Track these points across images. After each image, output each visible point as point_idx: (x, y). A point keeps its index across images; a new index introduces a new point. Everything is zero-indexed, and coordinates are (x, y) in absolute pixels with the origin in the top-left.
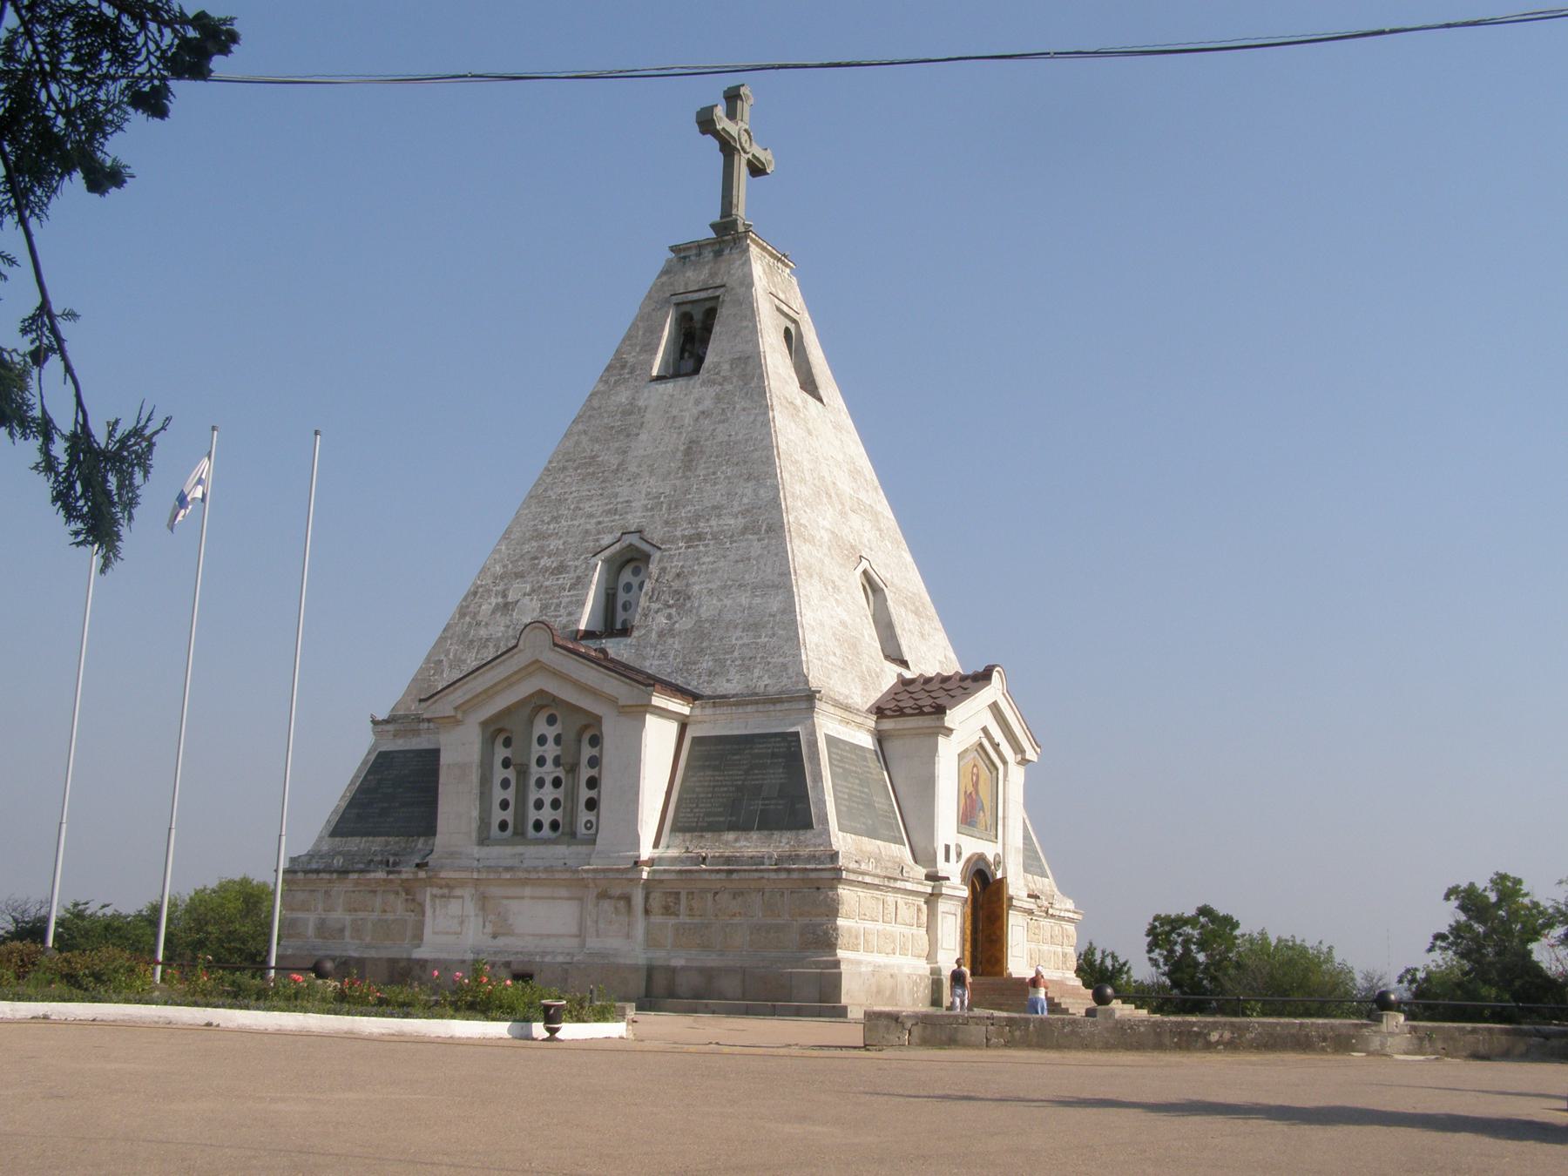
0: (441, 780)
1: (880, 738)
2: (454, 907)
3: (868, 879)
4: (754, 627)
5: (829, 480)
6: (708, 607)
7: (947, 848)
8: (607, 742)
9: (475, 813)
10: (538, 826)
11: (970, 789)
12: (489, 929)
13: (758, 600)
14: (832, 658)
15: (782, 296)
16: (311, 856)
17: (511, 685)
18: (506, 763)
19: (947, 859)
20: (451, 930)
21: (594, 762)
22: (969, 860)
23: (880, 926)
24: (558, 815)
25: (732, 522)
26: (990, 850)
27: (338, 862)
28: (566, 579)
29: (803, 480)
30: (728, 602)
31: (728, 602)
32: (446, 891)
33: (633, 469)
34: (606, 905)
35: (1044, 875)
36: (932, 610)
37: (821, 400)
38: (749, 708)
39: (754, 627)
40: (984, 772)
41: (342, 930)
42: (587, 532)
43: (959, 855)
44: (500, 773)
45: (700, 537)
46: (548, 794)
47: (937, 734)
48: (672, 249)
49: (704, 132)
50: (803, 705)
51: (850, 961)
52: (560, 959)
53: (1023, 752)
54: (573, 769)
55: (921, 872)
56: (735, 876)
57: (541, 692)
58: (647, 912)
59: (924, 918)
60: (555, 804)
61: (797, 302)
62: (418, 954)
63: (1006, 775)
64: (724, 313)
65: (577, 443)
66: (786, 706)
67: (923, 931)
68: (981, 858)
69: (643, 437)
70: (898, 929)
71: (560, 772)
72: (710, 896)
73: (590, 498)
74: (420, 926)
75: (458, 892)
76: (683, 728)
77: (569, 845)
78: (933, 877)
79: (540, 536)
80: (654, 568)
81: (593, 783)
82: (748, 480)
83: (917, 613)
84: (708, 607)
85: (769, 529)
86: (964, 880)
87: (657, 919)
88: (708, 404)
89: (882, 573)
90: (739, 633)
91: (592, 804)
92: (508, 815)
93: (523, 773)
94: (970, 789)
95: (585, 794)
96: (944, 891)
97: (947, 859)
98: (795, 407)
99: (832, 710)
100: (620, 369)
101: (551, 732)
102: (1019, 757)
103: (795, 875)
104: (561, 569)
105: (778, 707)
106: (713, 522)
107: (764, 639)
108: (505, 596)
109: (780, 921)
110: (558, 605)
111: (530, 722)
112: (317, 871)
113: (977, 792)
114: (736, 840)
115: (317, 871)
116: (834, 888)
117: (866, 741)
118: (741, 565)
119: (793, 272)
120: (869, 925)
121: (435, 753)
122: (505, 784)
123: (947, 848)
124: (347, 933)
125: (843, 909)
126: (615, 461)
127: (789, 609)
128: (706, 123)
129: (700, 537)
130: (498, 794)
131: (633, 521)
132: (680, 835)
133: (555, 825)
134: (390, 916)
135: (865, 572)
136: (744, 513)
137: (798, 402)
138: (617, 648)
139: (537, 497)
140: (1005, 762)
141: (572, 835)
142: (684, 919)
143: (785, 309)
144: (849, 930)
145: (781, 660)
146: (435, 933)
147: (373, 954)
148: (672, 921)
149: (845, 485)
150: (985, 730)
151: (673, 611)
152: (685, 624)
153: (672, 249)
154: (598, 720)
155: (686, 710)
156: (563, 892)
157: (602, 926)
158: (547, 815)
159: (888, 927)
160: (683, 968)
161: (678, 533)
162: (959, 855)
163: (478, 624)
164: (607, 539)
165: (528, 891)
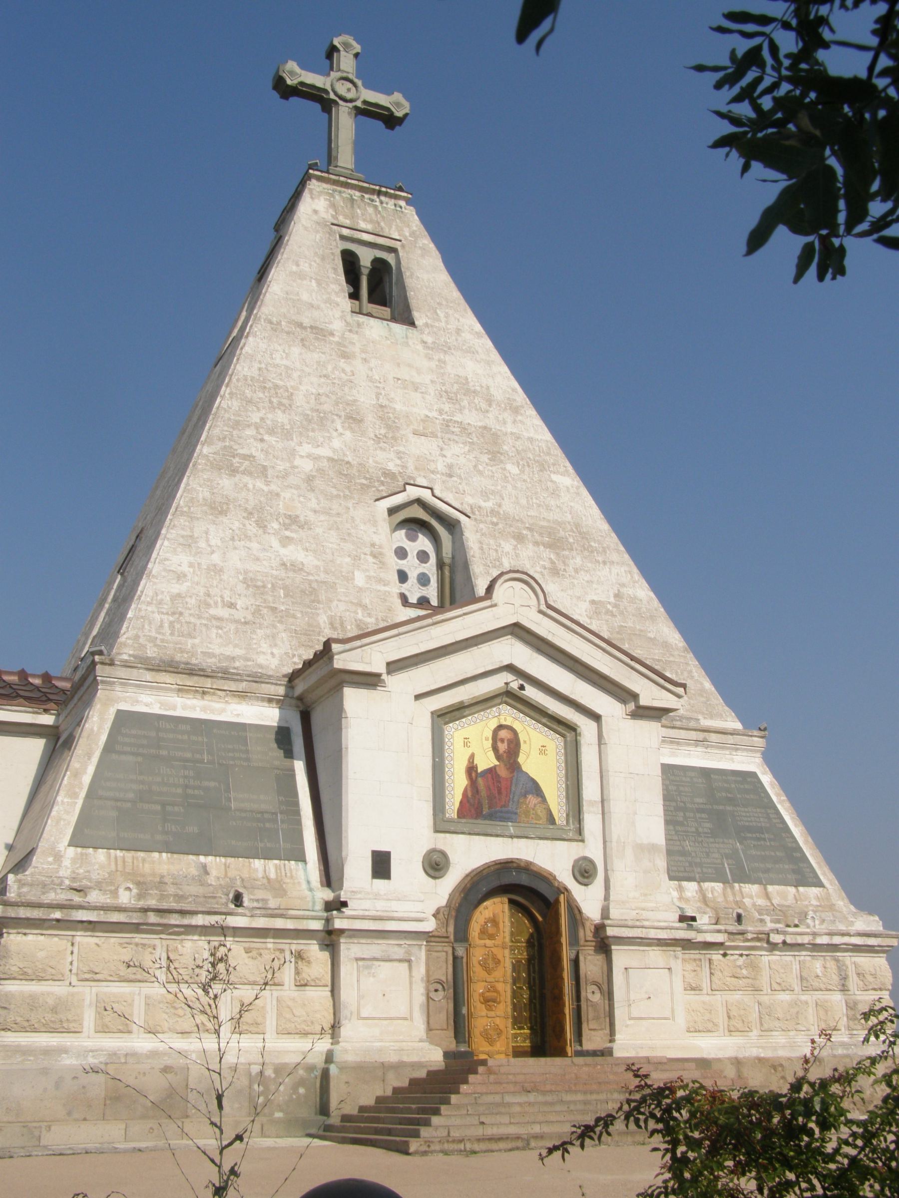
11: (486, 761)
15: (363, 225)
29: (286, 408)
36: (613, 540)
53: (635, 696)
89: (449, 497)
94: (486, 761)
99: (149, 676)
102: (632, 706)
113: (514, 766)
119: (408, 202)
137: (337, 326)
155: (48, 719)
162: (435, 865)
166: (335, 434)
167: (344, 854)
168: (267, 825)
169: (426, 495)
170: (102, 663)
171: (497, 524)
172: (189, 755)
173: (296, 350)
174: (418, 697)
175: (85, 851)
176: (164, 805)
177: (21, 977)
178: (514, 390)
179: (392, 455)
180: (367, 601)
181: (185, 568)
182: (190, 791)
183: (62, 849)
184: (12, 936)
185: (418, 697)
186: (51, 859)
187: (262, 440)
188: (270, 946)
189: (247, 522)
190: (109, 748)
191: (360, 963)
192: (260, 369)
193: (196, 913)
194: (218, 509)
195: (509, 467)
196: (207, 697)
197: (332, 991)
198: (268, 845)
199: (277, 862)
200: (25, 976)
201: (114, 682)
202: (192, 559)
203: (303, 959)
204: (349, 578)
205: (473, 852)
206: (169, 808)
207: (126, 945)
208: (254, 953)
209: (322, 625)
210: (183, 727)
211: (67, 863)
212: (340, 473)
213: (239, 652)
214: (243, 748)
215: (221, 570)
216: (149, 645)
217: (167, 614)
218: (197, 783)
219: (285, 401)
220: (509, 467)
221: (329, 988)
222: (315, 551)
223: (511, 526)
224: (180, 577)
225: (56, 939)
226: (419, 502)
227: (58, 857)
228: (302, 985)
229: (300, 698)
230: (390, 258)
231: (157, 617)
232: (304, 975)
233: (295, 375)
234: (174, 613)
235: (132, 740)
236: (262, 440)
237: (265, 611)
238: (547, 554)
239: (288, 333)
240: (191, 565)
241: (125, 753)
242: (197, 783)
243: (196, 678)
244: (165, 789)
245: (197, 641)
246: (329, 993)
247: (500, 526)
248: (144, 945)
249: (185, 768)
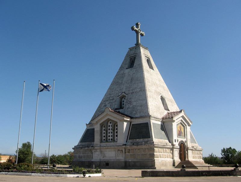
0: (95, 133)
2: (97, 153)
4: (141, 106)
5: (154, 82)
6: (134, 104)
7: (175, 140)
8: (118, 126)
9: (100, 138)
10: (109, 139)
12: (102, 156)
14: (154, 110)
15: (146, 54)
16: (77, 146)
17: (104, 118)
18: (104, 130)
19: (175, 142)
20: (97, 156)
21: (117, 129)
22: (180, 142)
23: (163, 153)
24: (112, 138)
25: (138, 90)
26: (184, 140)
27: (81, 146)
28: (114, 101)
29: (149, 82)
30: (137, 102)
31: (137, 102)
32: (96, 150)
33: (123, 83)
34: (119, 152)
35: (196, 143)
36: (174, 102)
37: (153, 70)
39: (141, 106)
40: (182, 127)
41: (82, 157)
42: (117, 93)
43: (178, 141)
44: (104, 132)
45: (133, 92)
46: (110, 134)
48: (129, 49)
49: (132, 30)
50: (149, 118)
51: (157, 160)
52: (113, 161)
54: (114, 130)
57: (108, 118)
58: (125, 153)
60: (112, 136)
61: (149, 55)
62: (93, 160)
63: (186, 128)
64: (137, 57)
65: (116, 80)
67: (171, 154)
68: (182, 141)
70: (166, 154)
71: (112, 131)
72: (135, 150)
73: (117, 88)
74: (93, 156)
75: (97, 151)
77: (113, 142)
79: (110, 94)
80: (126, 98)
81: (117, 132)
82: (140, 83)
83: (171, 102)
84: (134, 104)
85: (143, 90)
86: (179, 145)
87: (127, 154)
88: (134, 72)
89: (165, 96)
90: (139, 107)
91: (117, 136)
92: (105, 138)
93: (107, 131)
94: (179, 130)
95: (116, 134)
97: (175, 142)
98: (149, 71)
100: (121, 68)
101: (111, 125)
103: (147, 146)
104: (113, 99)
106: (135, 90)
107: (143, 108)
108: (105, 104)
109: (145, 153)
111: (107, 123)
112: (78, 148)
113: (181, 130)
115: (78, 148)
120: (161, 153)
121: (94, 129)
122: (104, 133)
123: (175, 140)
124: (83, 157)
125: (155, 151)
128: (132, 29)
129: (133, 92)
130: (103, 135)
131: (124, 91)
133: (112, 139)
134: (88, 155)
135: (161, 96)
136: (140, 88)
137: (149, 70)
138: (121, 110)
139: (110, 88)
140: (186, 125)
141: (114, 141)
142: (131, 153)
143: (147, 56)
145: (145, 111)
146: (95, 157)
147: (86, 160)
148: (129, 154)
149: (158, 82)
150: (181, 120)
152: (131, 106)
153: (129, 49)
154: (117, 122)
156: (113, 150)
157: (118, 155)
158: (110, 138)
159: (164, 154)
160: (131, 162)
162: (178, 141)
163: (101, 109)
164: (120, 94)
165: (108, 150)
205: (180, 140)
238: (171, 103)
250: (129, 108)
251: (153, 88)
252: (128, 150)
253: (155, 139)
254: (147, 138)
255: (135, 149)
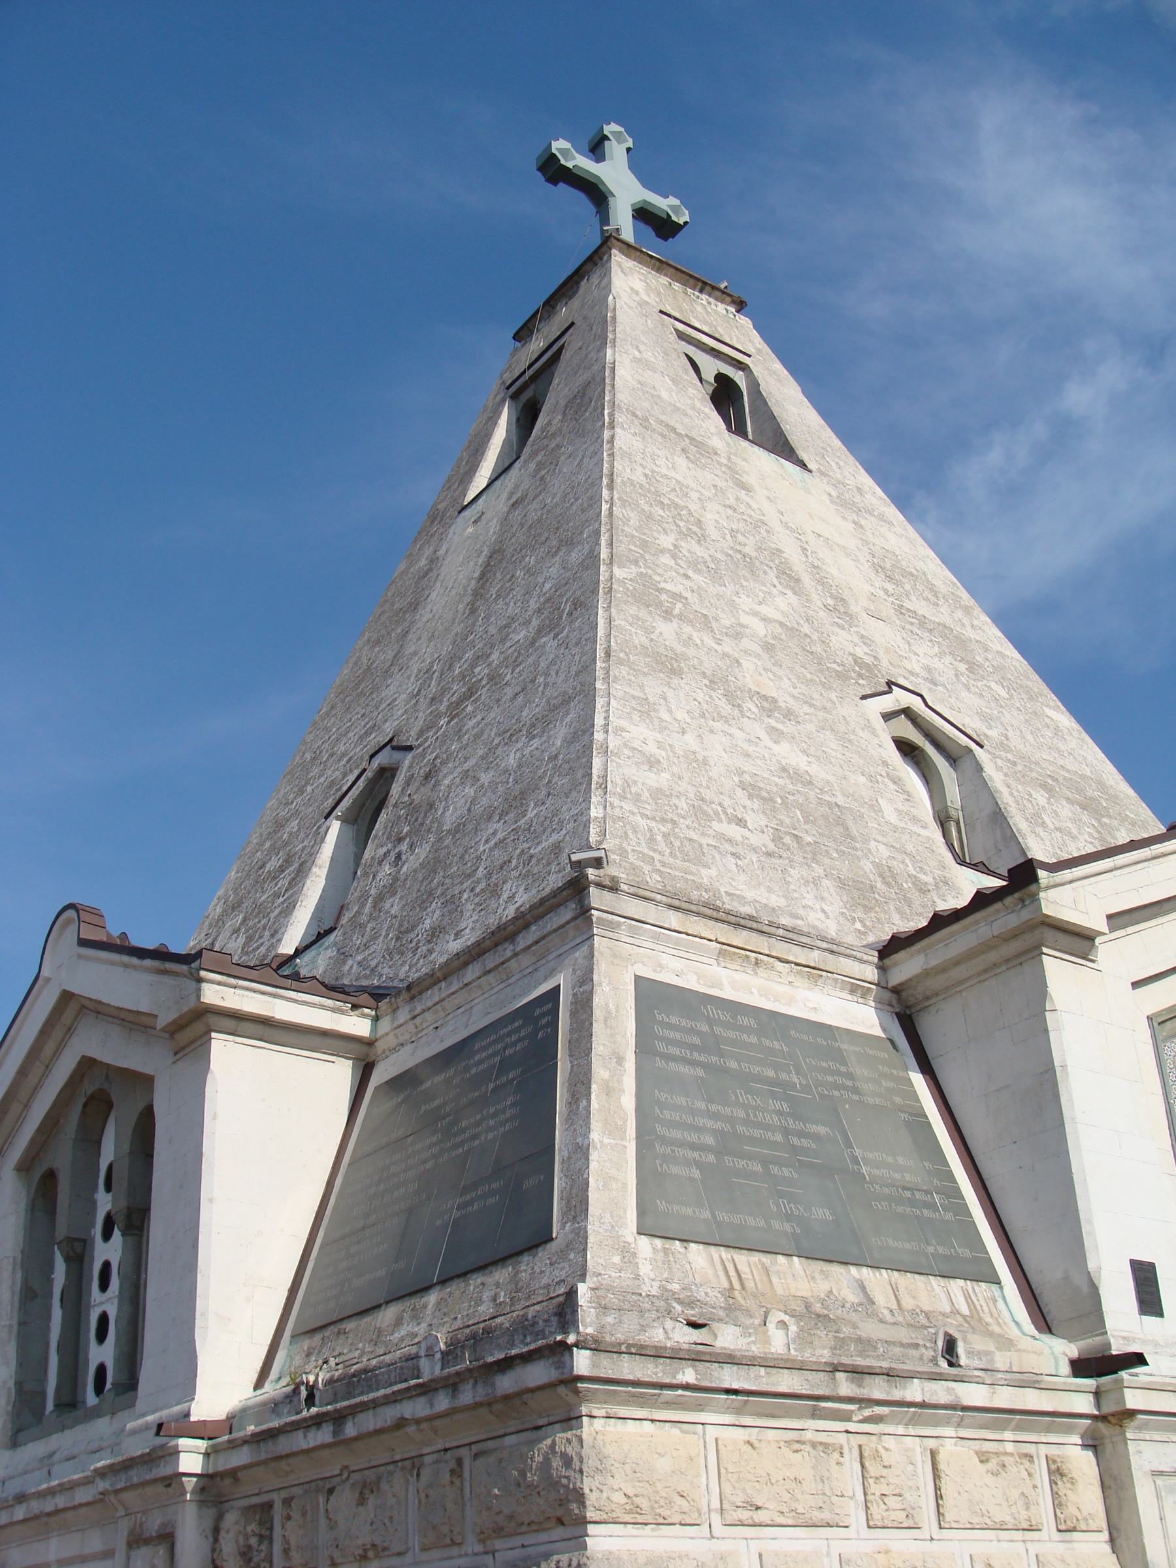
1: (907, 1012)
3: (729, 1377)
4: (516, 802)
13: (536, 743)
30: (485, 778)
37: (803, 465)
38: (471, 973)
47: (1034, 952)
50: (567, 913)
55: (1060, 1351)
56: (350, 1430)
59: (1087, 1498)
66: (534, 932)
69: (433, 595)
76: (365, 1070)
78: (1100, 1365)
85: (577, 604)
89: (960, 709)
90: (493, 826)
96: (1133, 1400)
99: (674, 919)
104: (288, 862)
105: (523, 941)
110: (264, 928)
114: (398, 1322)
116: (571, 1420)
117: (866, 1018)
118: (520, 699)
126: (390, 654)
127: (582, 735)
132: (306, 1344)
144: (608, 1556)
145: (555, 837)
149: (858, 581)
151: (404, 847)
154: (146, 1082)
155: (358, 1025)
161: (443, 708)
166: (774, 591)
167: (1091, 1265)
168: (926, 1212)
169: (916, 703)
170: (599, 885)
171: (1014, 764)
172: (771, 1073)
173: (682, 462)
174: (1136, 985)
175: (668, 1244)
176: (765, 1162)
177: (628, 1518)
178: (954, 584)
179: (856, 640)
180: (910, 848)
181: (652, 748)
182: (795, 1141)
183: (630, 1239)
184: (598, 1424)
185: (1136, 985)
186: (617, 1259)
187: (687, 577)
188: (1010, 1447)
189: (713, 694)
190: (644, 1048)
191: (1160, 1481)
192: (646, 475)
193: (911, 1375)
194: (669, 665)
195: (993, 685)
196: (761, 971)
197: (1112, 1540)
198: (941, 1250)
199: (961, 1282)
200: (635, 1517)
201: (619, 924)
202: (659, 737)
203: (1062, 1475)
204: (875, 808)
206: (775, 1170)
207: (797, 1446)
208: (993, 1464)
209: (871, 876)
210: (745, 1021)
211: (645, 1269)
212: (804, 650)
213: (782, 902)
214: (843, 1069)
215: (705, 762)
216: (647, 868)
217: (653, 819)
218: (799, 1125)
219: (695, 529)
220: (993, 685)
221: (1105, 1535)
222: (818, 758)
223: (1031, 770)
224: (652, 763)
225: (675, 1431)
226: (907, 712)
227: (629, 1254)
228: (1066, 1529)
229: (897, 991)
230: (739, 377)
231: (642, 822)
232: (1071, 1510)
233: (694, 495)
234: (664, 821)
235: (677, 1035)
236: (687, 577)
237: (787, 840)
239: (664, 436)
240: (660, 745)
241: (674, 1059)
242: (799, 1125)
243: (745, 933)
244: (757, 1133)
245: (713, 872)
246: (1107, 1548)
247: (1019, 768)
248: (826, 1445)
249: (773, 1095)
250: (391, 889)
251: (745, 602)
252: (248, 1511)
253: (645, 1246)
254: (501, 1261)
255: (331, 1491)
